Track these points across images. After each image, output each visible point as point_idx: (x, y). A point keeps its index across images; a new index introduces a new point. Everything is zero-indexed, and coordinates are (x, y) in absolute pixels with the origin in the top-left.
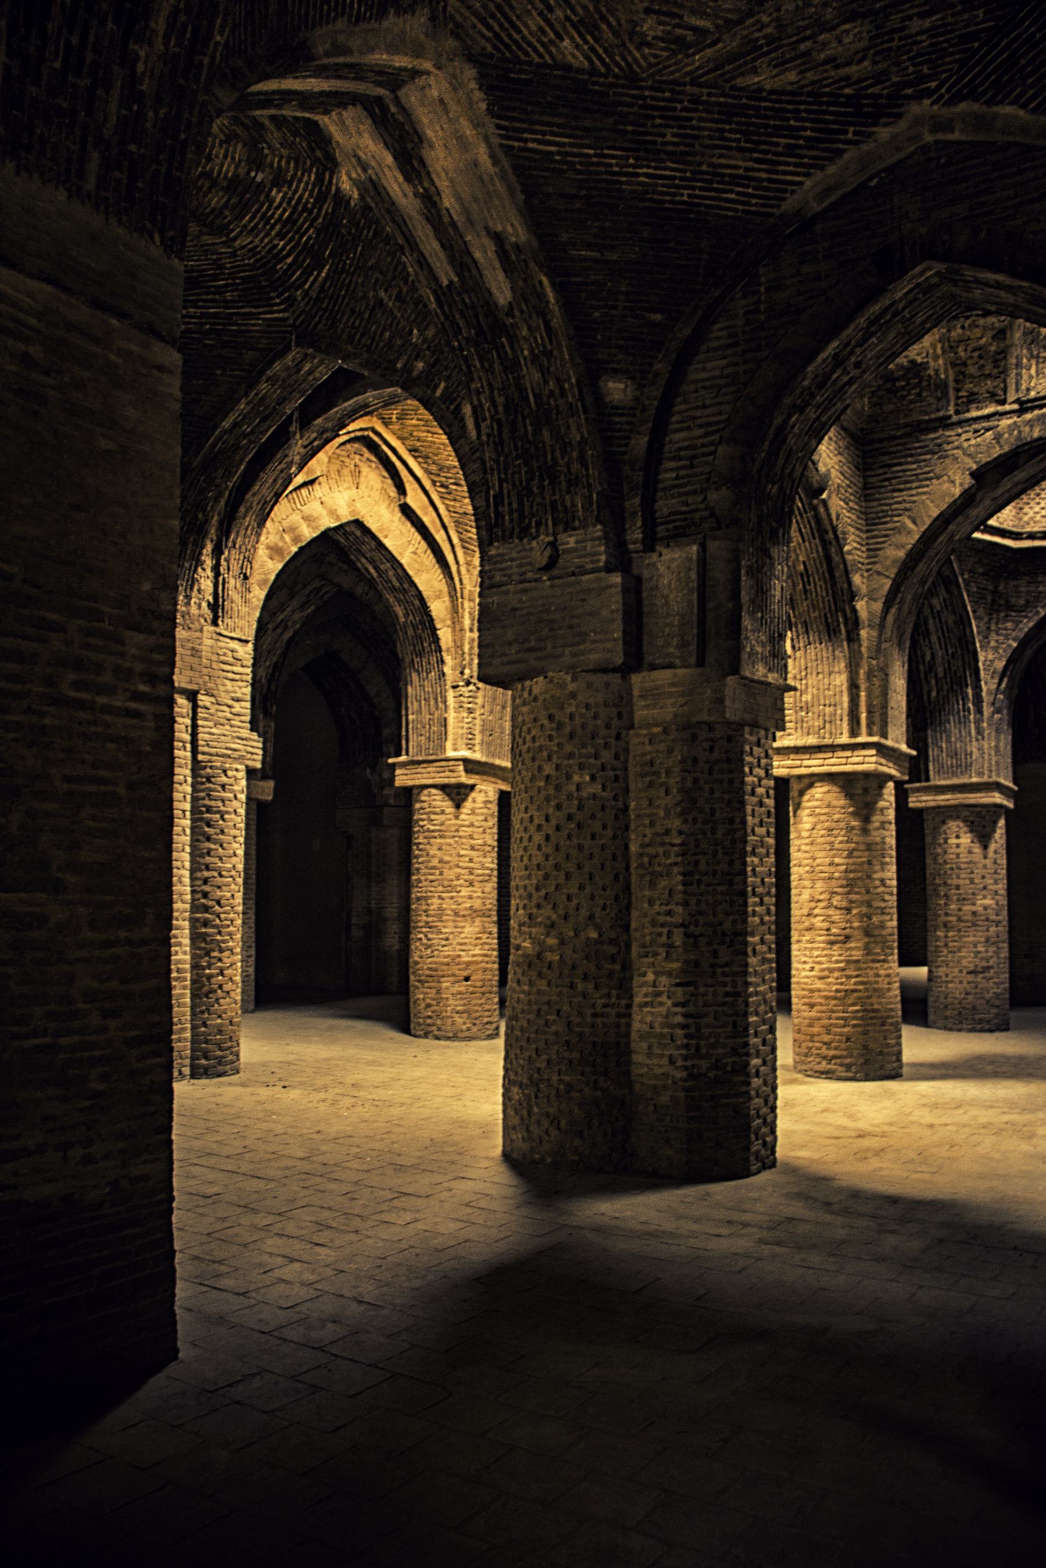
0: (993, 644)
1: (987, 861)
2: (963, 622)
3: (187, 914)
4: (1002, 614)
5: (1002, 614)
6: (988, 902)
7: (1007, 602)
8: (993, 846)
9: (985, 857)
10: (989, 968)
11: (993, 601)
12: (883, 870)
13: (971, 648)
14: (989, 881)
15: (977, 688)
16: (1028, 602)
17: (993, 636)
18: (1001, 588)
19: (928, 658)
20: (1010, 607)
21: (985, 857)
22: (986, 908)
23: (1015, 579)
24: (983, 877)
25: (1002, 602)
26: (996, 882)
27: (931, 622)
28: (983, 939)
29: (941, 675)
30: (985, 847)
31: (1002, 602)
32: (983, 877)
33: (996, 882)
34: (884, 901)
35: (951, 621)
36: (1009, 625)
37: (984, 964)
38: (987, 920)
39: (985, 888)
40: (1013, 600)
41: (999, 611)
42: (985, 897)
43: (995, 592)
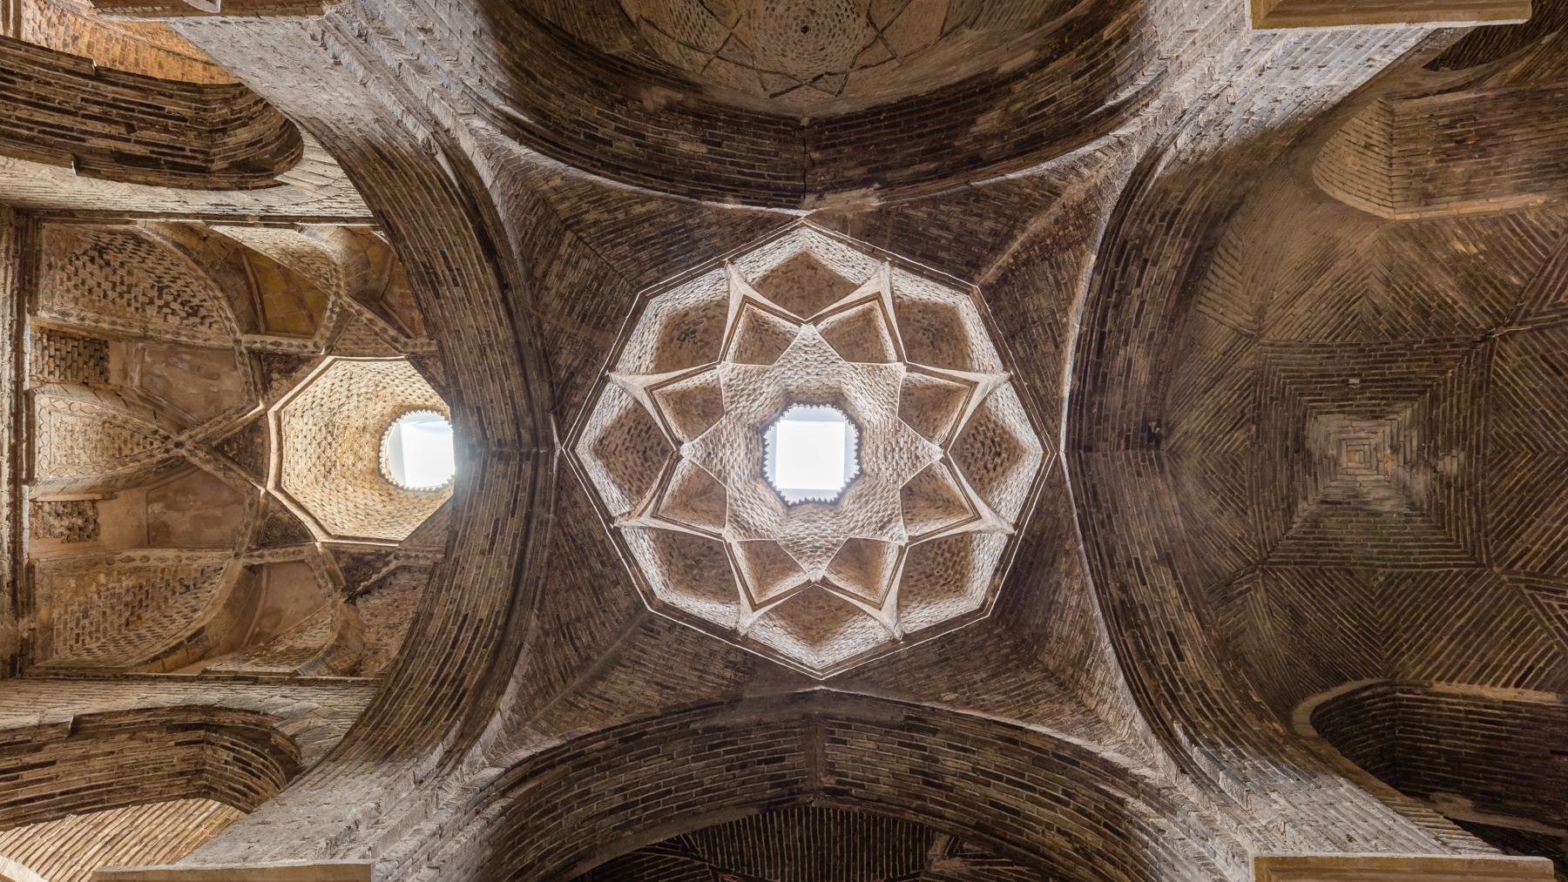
0: (1111, 719)
2: (1012, 740)
4: (1083, 679)
11: (1060, 685)
13: (1067, 753)
15: (1135, 784)
16: (1082, 630)
17: (1103, 709)
18: (1052, 664)
19: (1061, 841)
20: (1079, 663)
23: (1047, 637)
25: (1070, 671)
27: (993, 793)
29: (1099, 843)
35: (1000, 760)
36: (1099, 675)
43: (1050, 675)
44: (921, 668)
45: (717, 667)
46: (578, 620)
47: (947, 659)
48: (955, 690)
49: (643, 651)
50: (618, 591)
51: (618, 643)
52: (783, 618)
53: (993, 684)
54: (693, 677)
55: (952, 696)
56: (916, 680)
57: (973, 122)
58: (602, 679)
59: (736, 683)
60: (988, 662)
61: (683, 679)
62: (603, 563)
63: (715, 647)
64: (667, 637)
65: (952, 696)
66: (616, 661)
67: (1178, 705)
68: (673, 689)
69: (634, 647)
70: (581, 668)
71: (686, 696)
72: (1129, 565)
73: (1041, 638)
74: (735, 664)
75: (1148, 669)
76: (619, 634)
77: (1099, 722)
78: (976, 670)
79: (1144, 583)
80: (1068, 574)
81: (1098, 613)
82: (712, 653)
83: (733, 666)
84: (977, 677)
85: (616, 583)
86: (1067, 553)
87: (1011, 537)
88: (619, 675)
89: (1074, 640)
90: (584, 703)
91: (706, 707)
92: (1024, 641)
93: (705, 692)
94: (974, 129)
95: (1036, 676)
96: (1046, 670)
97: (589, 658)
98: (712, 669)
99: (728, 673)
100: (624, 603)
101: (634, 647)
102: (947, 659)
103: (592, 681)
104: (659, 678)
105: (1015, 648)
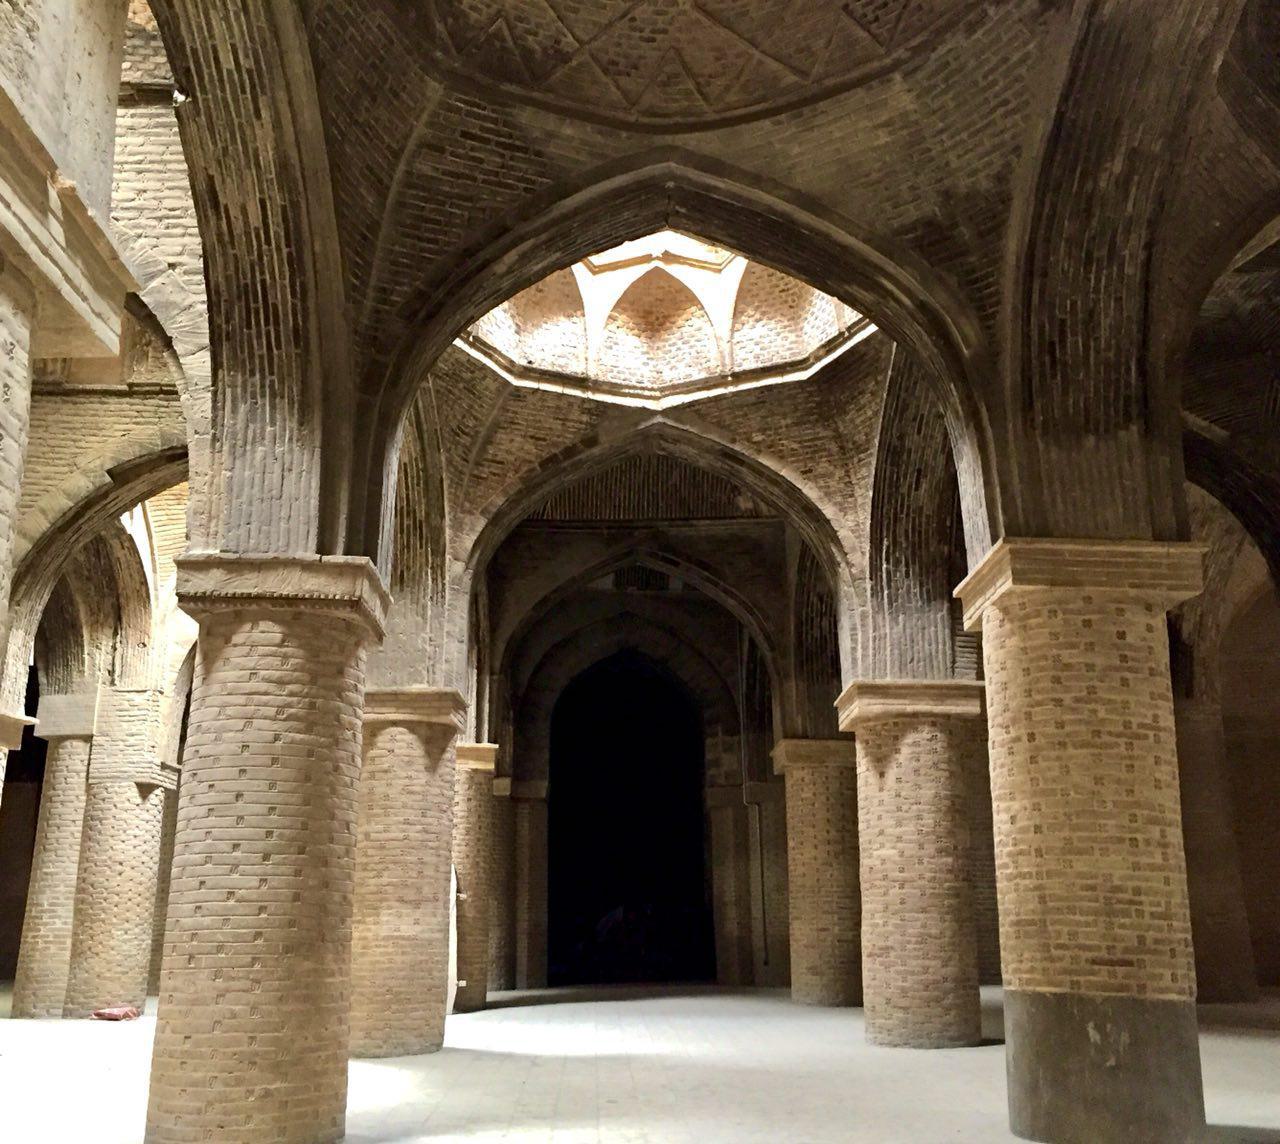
1: (885, 795)
3: (73, 895)
4: (856, 460)
5: (856, 460)
6: (888, 852)
7: (854, 443)
8: (892, 773)
9: (881, 790)
10: (887, 949)
11: (842, 448)
12: (369, 822)
14: (888, 822)
16: (866, 435)
21: (881, 790)
22: (883, 862)
23: (846, 413)
24: (880, 818)
26: (899, 824)
28: (880, 907)
30: (882, 775)
31: (850, 446)
32: (880, 818)
33: (899, 824)
34: (366, 856)
37: (881, 944)
38: (885, 878)
39: (881, 833)
40: (856, 438)
41: (852, 457)
42: (882, 846)
43: (838, 437)
44: (741, 407)
45: (575, 415)
46: (464, 417)
47: (764, 402)
48: (763, 431)
49: (516, 413)
50: (488, 381)
51: (495, 412)
52: (625, 310)
53: (795, 432)
54: (557, 425)
55: (758, 437)
56: (736, 417)
57: (849, 283)
58: (491, 443)
59: (593, 426)
60: (796, 410)
61: (550, 429)
62: (472, 372)
63: (571, 400)
64: (530, 399)
65: (758, 437)
66: (496, 426)
67: (895, 526)
68: (544, 440)
69: (508, 411)
70: (473, 444)
71: (555, 445)
72: (914, 419)
73: (843, 411)
74: (589, 410)
75: (890, 495)
76: (493, 406)
77: (852, 496)
78: (785, 416)
79: (919, 432)
80: (872, 393)
81: (876, 441)
82: (571, 404)
83: (589, 412)
84: (783, 422)
85: (484, 378)
86: (877, 383)
87: (841, 334)
88: (501, 436)
89: (859, 432)
90: (485, 472)
91: (570, 452)
92: (828, 401)
93: (569, 439)
94: (847, 287)
95: (829, 433)
96: (836, 430)
97: (477, 432)
98: (571, 417)
99: (585, 418)
100: (493, 386)
101: (508, 411)
102: (764, 402)
103: (483, 449)
104: (532, 432)
105: (819, 404)
